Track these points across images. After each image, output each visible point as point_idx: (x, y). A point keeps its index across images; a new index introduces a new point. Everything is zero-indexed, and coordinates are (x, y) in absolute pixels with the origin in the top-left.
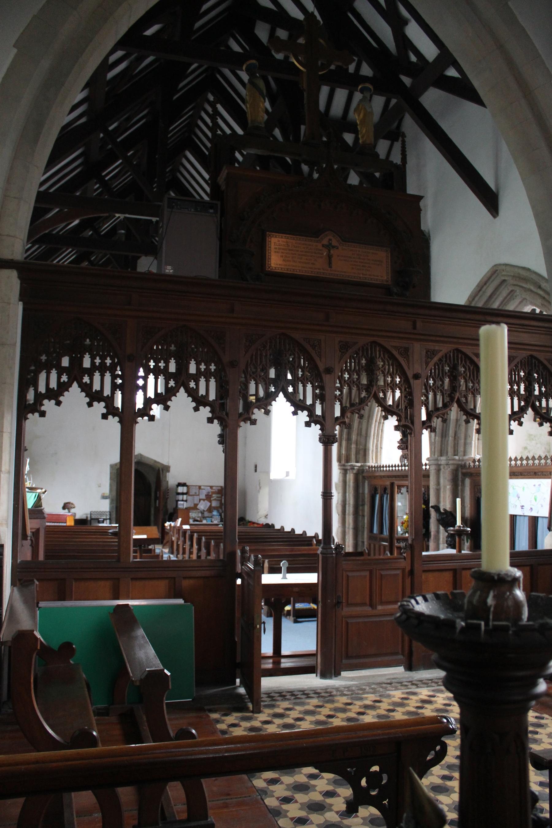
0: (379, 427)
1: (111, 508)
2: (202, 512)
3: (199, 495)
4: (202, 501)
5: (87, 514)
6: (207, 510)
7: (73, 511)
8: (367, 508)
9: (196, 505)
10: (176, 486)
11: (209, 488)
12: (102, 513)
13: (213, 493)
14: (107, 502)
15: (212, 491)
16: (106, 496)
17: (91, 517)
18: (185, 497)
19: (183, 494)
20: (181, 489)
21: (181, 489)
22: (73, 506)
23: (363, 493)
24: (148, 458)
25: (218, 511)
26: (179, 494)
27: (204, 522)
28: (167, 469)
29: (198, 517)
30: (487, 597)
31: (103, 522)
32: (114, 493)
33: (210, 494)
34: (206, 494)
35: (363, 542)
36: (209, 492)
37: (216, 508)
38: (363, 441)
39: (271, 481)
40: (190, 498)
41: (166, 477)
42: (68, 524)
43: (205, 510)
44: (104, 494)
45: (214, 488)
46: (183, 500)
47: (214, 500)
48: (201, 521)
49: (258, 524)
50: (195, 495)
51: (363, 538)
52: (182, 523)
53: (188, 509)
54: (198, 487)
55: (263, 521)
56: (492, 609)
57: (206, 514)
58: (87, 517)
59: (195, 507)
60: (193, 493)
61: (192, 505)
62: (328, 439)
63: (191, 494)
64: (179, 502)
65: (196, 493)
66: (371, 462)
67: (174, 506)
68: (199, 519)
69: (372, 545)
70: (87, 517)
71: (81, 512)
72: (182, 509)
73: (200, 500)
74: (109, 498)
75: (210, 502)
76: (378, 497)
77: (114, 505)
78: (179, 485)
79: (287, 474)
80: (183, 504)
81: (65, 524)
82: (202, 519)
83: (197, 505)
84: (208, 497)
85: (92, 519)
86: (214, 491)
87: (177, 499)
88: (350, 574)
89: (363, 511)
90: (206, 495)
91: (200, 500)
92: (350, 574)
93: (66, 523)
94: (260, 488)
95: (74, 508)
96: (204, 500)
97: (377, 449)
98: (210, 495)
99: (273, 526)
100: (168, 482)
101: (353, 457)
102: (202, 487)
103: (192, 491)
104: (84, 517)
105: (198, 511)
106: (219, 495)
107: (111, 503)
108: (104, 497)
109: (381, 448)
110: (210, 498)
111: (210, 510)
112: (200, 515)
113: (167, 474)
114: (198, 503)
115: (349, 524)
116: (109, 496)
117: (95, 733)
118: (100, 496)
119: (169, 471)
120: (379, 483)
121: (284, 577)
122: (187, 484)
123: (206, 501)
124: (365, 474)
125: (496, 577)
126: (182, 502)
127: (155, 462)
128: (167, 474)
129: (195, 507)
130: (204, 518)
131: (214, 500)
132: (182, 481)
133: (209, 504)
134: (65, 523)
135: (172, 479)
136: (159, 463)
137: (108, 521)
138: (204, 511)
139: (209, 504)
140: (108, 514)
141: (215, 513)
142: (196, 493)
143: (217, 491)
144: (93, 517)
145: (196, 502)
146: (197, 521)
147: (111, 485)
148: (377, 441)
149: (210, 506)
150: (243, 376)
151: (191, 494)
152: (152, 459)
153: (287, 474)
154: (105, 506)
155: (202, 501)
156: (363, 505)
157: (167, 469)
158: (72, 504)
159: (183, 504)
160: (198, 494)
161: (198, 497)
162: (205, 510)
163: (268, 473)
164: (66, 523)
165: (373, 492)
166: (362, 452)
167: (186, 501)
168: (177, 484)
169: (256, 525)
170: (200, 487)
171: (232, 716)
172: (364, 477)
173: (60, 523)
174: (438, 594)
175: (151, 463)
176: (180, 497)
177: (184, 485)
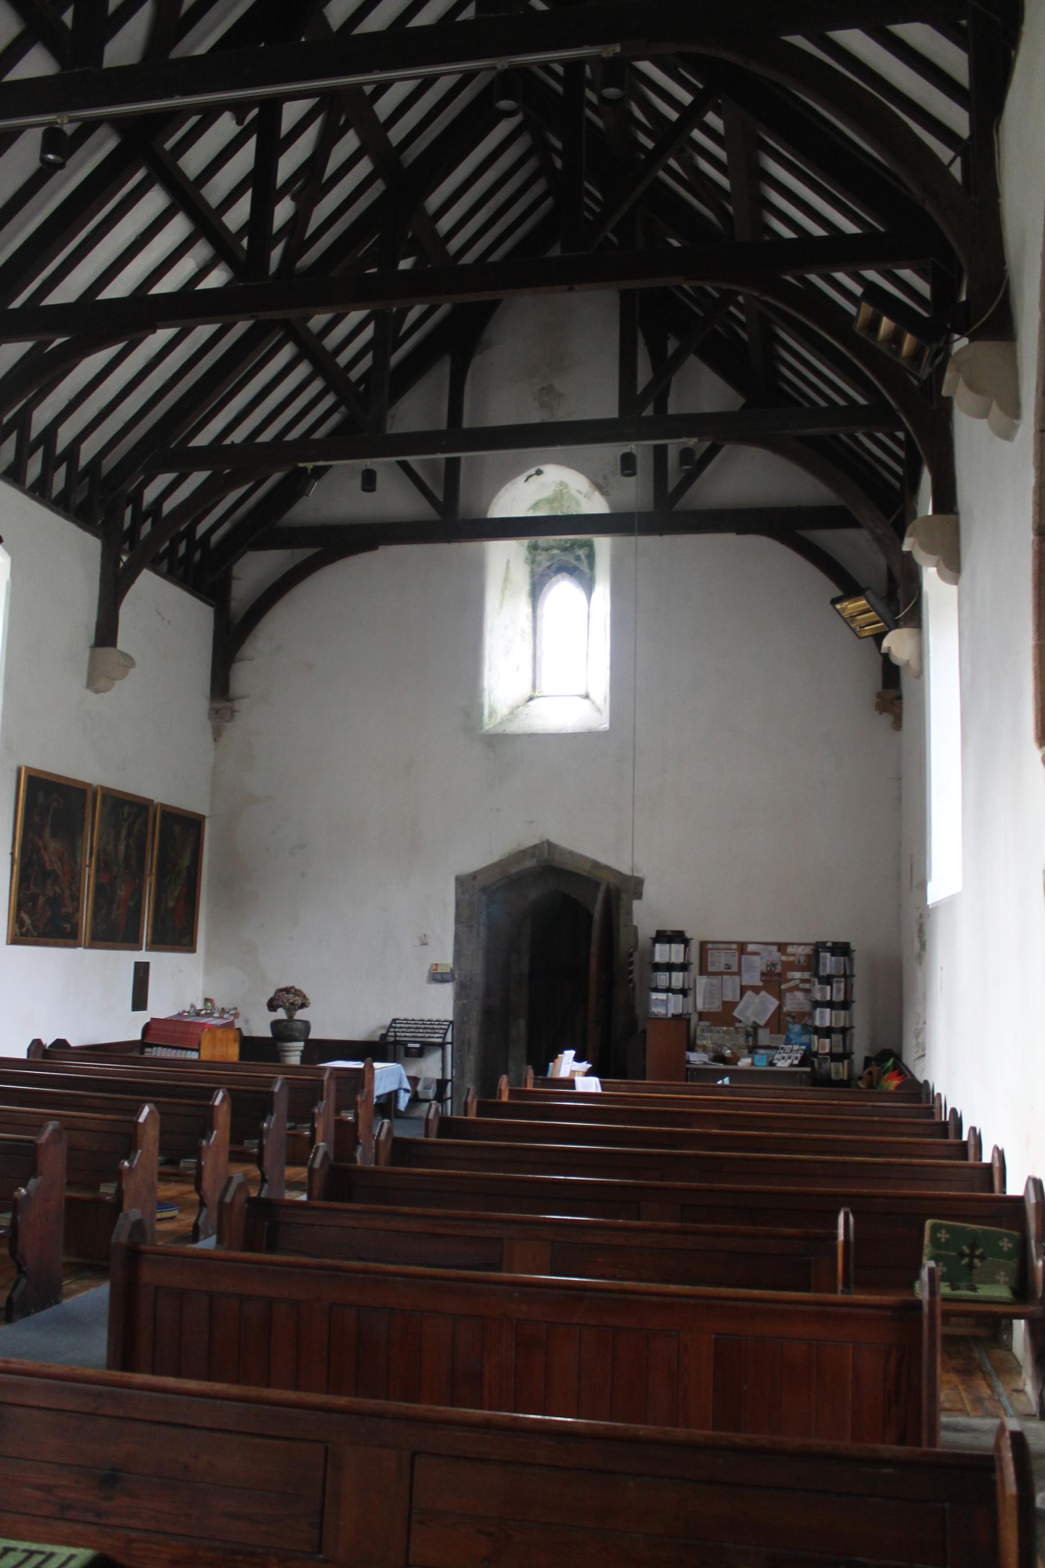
1: (461, 1010)
3: (739, 973)
4: (749, 993)
6: (766, 1026)
9: (729, 1006)
10: (650, 941)
11: (775, 948)
14: (448, 990)
15: (784, 958)
16: (442, 974)
18: (677, 979)
19: (670, 967)
20: (662, 953)
21: (662, 953)
22: (299, 1001)
24: (572, 854)
26: (658, 967)
28: (634, 886)
33: (779, 969)
34: (764, 968)
36: (774, 965)
40: (702, 981)
41: (630, 913)
42: (207, 1053)
43: (762, 1023)
45: (790, 950)
46: (669, 990)
47: (796, 988)
48: (734, 1060)
50: (728, 972)
54: (734, 946)
60: (722, 969)
61: (716, 1007)
63: (710, 969)
65: (728, 966)
68: (728, 1052)
73: (743, 990)
74: (453, 979)
75: (780, 996)
78: (664, 937)
80: (665, 1003)
81: (194, 1055)
83: (734, 1005)
86: (791, 959)
90: (763, 974)
91: (743, 990)
95: (303, 1006)
96: (756, 990)
98: (779, 974)
100: (636, 928)
102: (751, 948)
103: (718, 960)
105: (738, 1025)
106: (806, 975)
107: (458, 996)
108: (437, 977)
111: (778, 1022)
112: (741, 1040)
113: (636, 903)
114: (738, 999)
116: (452, 972)
119: (639, 896)
122: (688, 935)
123: (763, 993)
126: (662, 996)
127: (596, 865)
128: (636, 903)
129: (724, 1016)
130: (752, 1050)
132: (672, 925)
133: (773, 1004)
134: (193, 1050)
136: (607, 868)
138: (756, 1027)
139: (773, 1004)
142: (728, 966)
143: (802, 959)
144: (402, 1036)
145: (729, 997)
149: (780, 1007)
151: (710, 969)
155: (749, 993)
157: (634, 886)
158: (298, 993)
160: (733, 970)
161: (737, 978)
162: (762, 1023)
167: (684, 992)
168: (653, 935)
170: (742, 948)
175: (584, 870)
176: (662, 978)
177: (678, 937)
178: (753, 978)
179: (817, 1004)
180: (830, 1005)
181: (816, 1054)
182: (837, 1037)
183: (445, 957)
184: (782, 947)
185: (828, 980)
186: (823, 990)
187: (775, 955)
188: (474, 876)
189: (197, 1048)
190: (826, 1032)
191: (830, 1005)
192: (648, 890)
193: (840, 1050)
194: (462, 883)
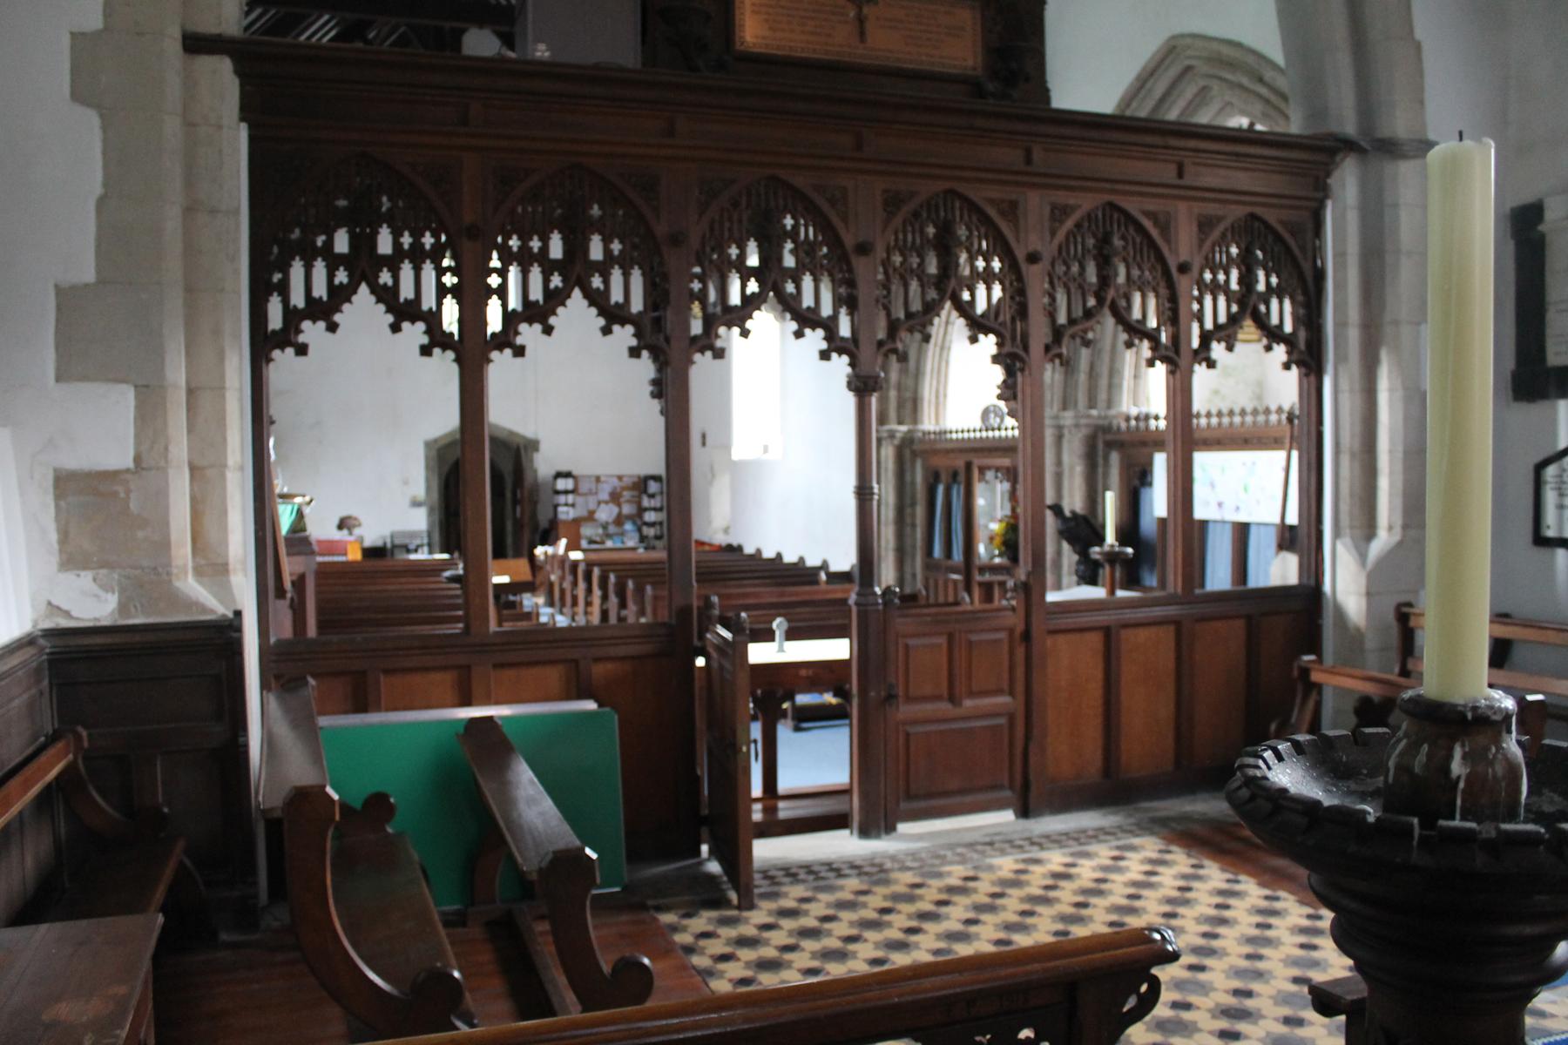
0: (941, 355)
2: (605, 526)
3: (596, 493)
4: (603, 506)
5: (384, 538)
7: (357, 531)
8: (920, 511)
10: (551, 479)
12: (413, 535)
13: (623, 489)
17: (392, 542)
18: (570, 498)
19: (566, 492)
20: (562, 484)
21: (562, 484)
22: (357, 523)
23: (913, 483)
25: (634, 523)
26: (557, 492)
27: (609, 544)
28: (533, 445)
29: (597, 535)
30: (1450, 757)
31: (416, 551)
32: (435, 495)
35: (914, 575)
36: (615, 488)
37: (630, 517)
38: (910, 382)
39: (735, 463)
40: (579, 500)
41: (531, 461)
44: (415, 497)
45: (625, 479)
46: (566, 505)
48: (602, 543)
49: (710, 545)
50: (590, 493)
51: (913, 566)
52: (569, 548)
53: (577, 522)
55: (720, 539)
56: (1462, 785)
57: (612, 529)
58: (385, 544)
59: (590, 517)
62: (865, 384)
64: (561, 509)
66: (928, 424)
67: (550, 515)
68: (598, 539)
69: (931, 582)
70: (385, 544)
71: (373, 533)
72: (565, 522)
75: (619, 505)
76: (941, 489)
77: (436, 517)
78: (559, 475)
79: (766, 449)
80: (567, 513)
82: (604, 538)
84: (615, 498)
85: (394, 546)
87: (555, 502)
88: (912, 642)
89: (913, 516)
91: (599, 503)
92: (912, 642)
93: (345, 554)
94: (713, 476)
95: (360, 525)
96: (606, 503)
97: (937, 397)
99: (740, 548)
101: (892, 414)
102: (603, 479)
103: (583, 488)
104: (379, 543)
108: (416, 504)
109: (945, 396)
110: (618, 499)
111: (619, 521)
112: (600, 531)
115: (887, 541)
117: (456, 974)
118: (407, 501)
119: (537, 450)
120: (940, 462)
121: (781, 650)
122: (575, 472)
124: (915, 447)
125: (1469, 716)
127: (512, 433)
129: (590, 517)
130: (609, 536)
131: (628, 501)
132: (564, 468)
133: (615, 510)
135: (544, 465)
137: (426, 549)
138: (607, 523)
139: (615, 510)
140: (425, 535)
141: (628, 526)
142: (590, 490)
144: (397, 542)
145: (592, 506)
146: (595, 542)
147: (428, 480)
148: (938, 382)
150: (881, 270)
152: (504, 429)
153: (766, 449)
154: (418, 521)
155: (603, 506)
156: (913, 504)
157: (533, 445)
158: (356, 519)
159: (567, 513)
160: (594, 491)
161: (595, 497)
162: (610, 520)
163: (727, 447)
164: (345, 554)
165: (931, 480)
166: (909, 405)
167: (573, 505)
169: (707, 548)
170: (598, 479)
171: (701, 917)
172: (914, 454)
173: (333, 555)
174: (1298, 742)
176: (562, 499)
177: (568, 475)
178: (604, 496)
179: (646, 509)
180: (655, 509)
181: (647, 537)
182: (658, 527)
183: (419, 489)
184: (620, 478)
185: (652, 496)
186: (650, 502)
187: (616, 482)
188: (436, 441)
189: (344, 552)
190: (652, 525)
191: (655, 509)
192: (543, 447)
193: (658, 533)
194: (428, 445)
